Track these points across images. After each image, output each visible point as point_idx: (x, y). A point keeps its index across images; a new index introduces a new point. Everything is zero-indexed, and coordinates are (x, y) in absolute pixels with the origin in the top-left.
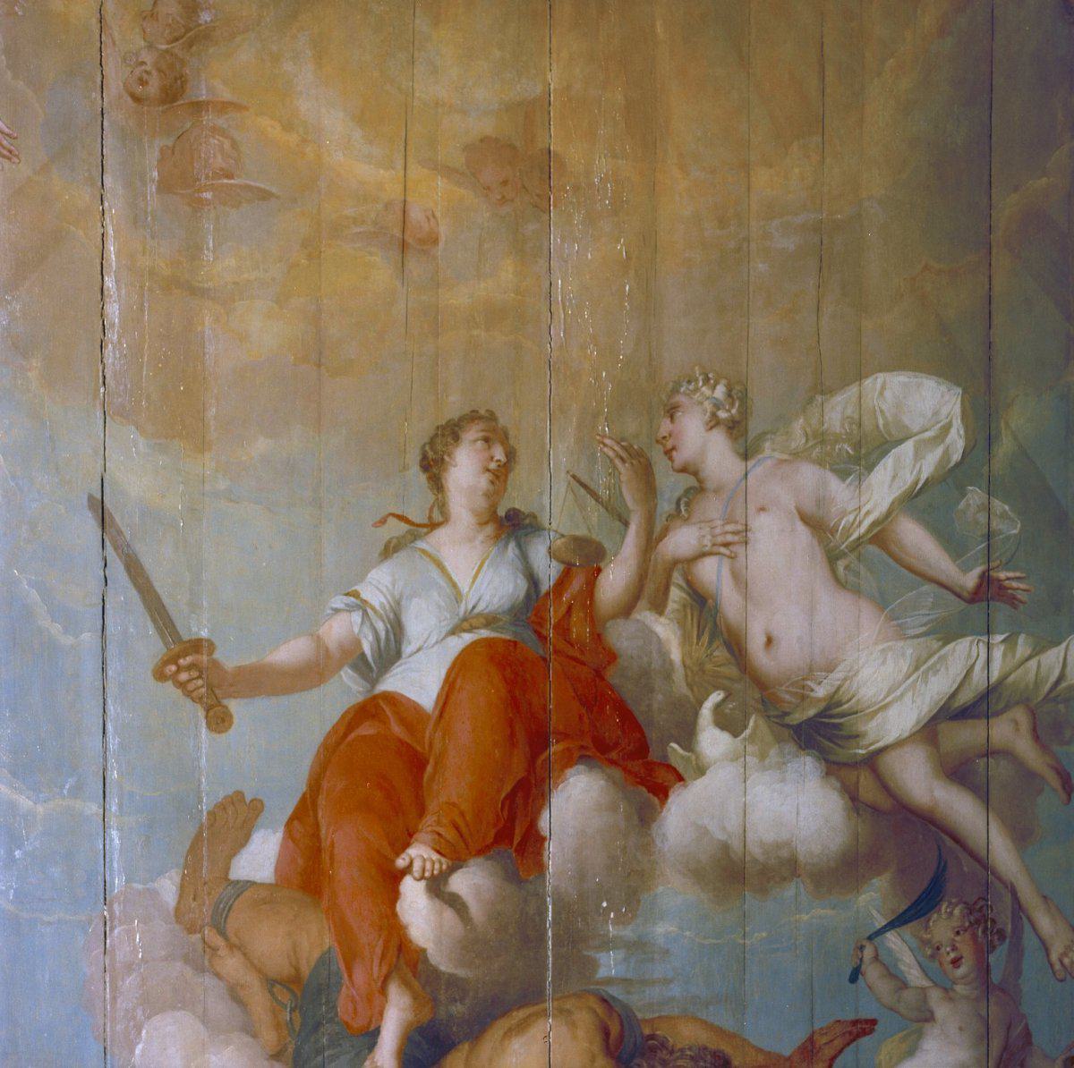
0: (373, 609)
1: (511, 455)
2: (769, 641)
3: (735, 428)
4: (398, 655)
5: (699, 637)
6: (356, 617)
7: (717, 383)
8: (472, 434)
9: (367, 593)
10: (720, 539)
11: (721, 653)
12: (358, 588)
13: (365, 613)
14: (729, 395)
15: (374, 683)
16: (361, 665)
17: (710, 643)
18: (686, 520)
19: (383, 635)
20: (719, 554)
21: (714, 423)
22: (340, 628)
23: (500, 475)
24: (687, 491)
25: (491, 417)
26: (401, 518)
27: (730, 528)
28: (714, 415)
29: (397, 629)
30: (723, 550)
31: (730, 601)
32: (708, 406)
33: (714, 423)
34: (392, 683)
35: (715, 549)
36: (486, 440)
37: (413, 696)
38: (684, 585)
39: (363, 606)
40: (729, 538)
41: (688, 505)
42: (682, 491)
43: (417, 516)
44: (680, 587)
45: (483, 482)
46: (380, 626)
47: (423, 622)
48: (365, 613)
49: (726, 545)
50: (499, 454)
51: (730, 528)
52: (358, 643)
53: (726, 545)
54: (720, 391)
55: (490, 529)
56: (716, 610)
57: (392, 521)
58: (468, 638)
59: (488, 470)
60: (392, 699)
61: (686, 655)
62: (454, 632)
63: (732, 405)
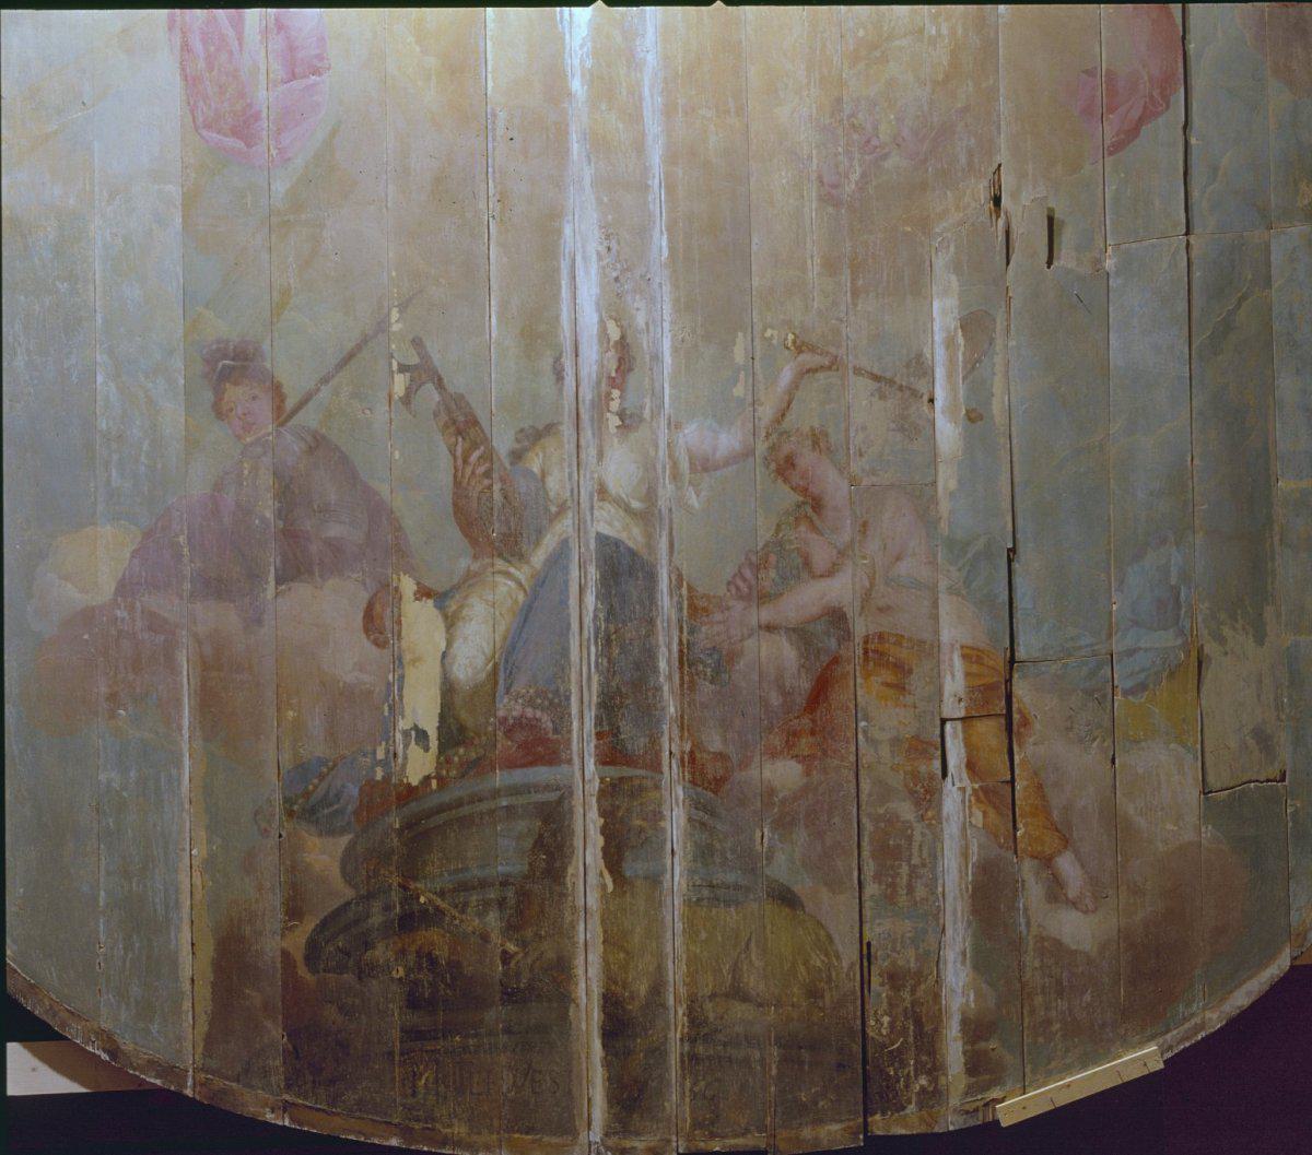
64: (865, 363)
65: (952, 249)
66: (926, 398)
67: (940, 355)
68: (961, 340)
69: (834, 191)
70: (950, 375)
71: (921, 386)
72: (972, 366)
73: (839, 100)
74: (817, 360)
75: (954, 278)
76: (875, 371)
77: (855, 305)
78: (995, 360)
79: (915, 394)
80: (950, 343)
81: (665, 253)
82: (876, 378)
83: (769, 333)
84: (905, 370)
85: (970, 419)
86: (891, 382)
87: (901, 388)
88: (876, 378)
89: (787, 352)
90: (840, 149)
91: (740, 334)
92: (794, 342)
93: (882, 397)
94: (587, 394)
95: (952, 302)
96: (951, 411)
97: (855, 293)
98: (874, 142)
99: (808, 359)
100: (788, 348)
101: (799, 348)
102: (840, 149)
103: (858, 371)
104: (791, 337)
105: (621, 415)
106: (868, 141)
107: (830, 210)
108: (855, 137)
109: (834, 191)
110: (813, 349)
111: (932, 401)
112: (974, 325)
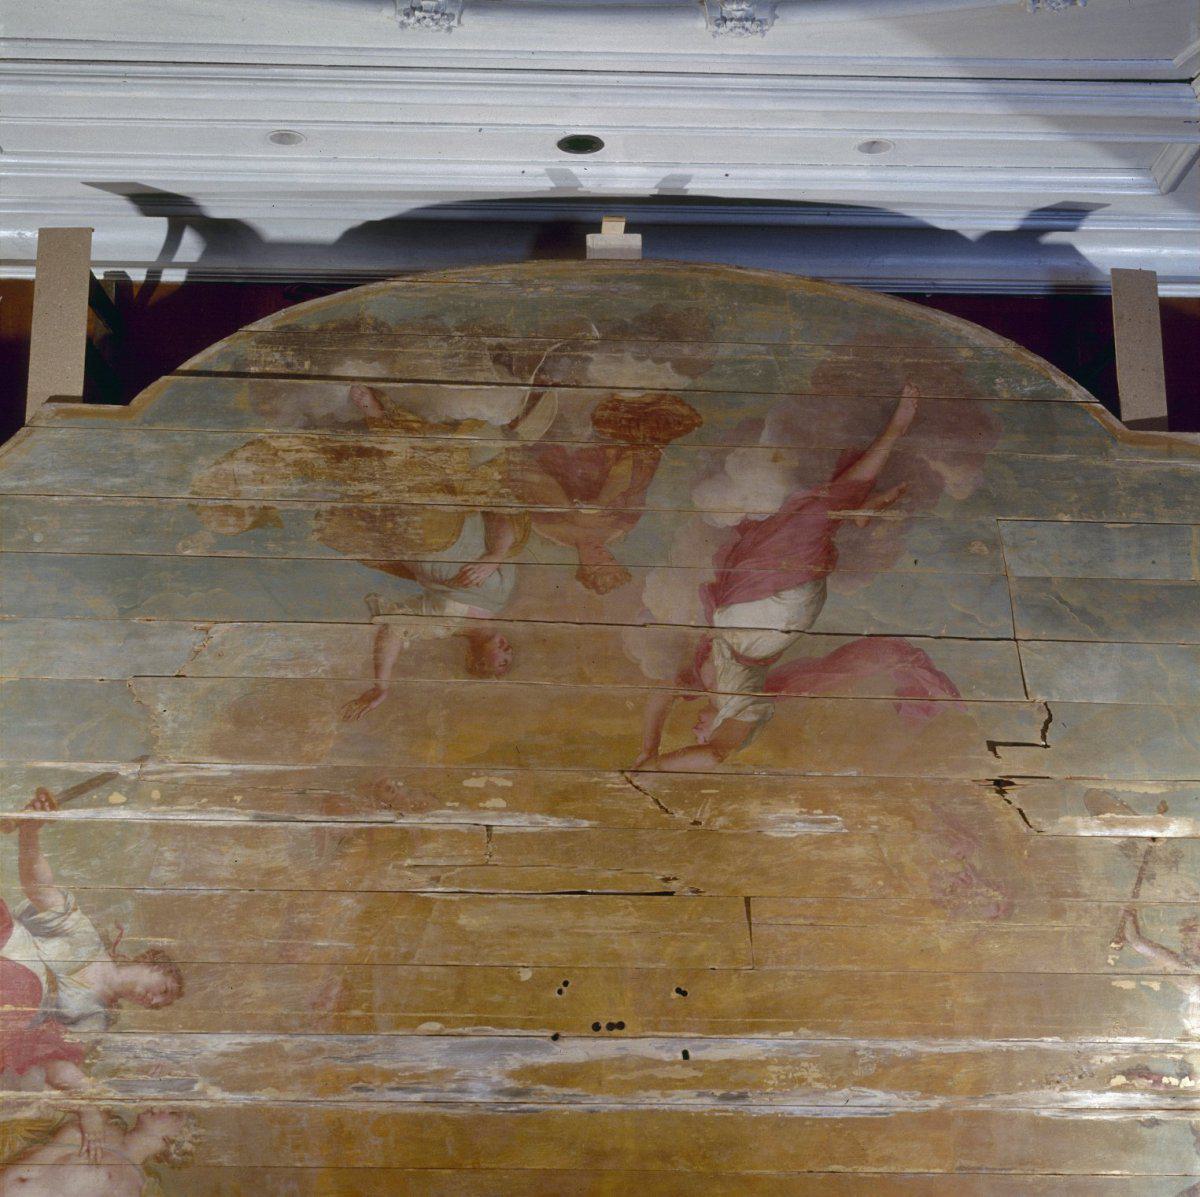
0: (65, 920)
1: (157, 1007)
2: (23, 1180)
3: (163, 1157)
4: (35, 935)
5: (29, 1131)
6: (61, 909)
7: (194, 1144)
8: (171, 983)
9: (75, 916)
10: (92, 1146)
11: (19, 1145)
12: (79, 911)
13: (63, 914)
14: (185, 1153)
15: (20, 919)
16: (31, 911)
17: (25, 1138)
18: (106, 1123)
19: (49, 925)
20: (83, 1145)
21: (168, 1141)
22: (56, 899)
23: (143, 1000)
24: (125, 1124)
25: (180, 994)
26: (121, 935)
27: (99, 1153)
28: (173, 1142)
29: (53, 934)
30: (85, 1148)
31: (52, 1153)
32: (178, 1139)
33: (168, 1141)
34: (18, 931)
35: (86, 1143)
36: (165, 992)
37: (11, 942)
38: (65, 1121)
39: (66, 913)
40: (92, 1153)
41: (116, 1124)
42: (125, 1120)
43: (120, 949)
44: (64, 1118)
45: (139, 989)
46: (55, 923)
47: (53, 949)
48: (63, 914)
49: (88, 1151)
50: (156, 1000)
51: (99, 1153)
52: (44, 909)
53: (88, 1151)
54: (188, 1146)
55: (110, 993)
56: (45, 1144)
57: (117, 933)
58: (43, 979)
59: (147, 992)
61: (18, 1121)
62: (49, 971)
63: (178, 1155)
64: (1129, 889)
65: (1040, 820)
66: (1151, 844)
67: (1119, 832)
68: (1108, 815)
69: (1002, 908)
70: (1135, 825)
71: (1142, 847)
72: (1126, 808)
73: (933, 902)
74: (1129, 925)
75: (1063, 819)
76: (1134, 881)
77: (1085, 896)
78: (1120, 790)
79: (1149, 852)
80: (1110, 824)
81: (1056, 1039)
82: (1139, 881)
83: (1111, 962)
84: (1132, 859)
85: (1165, 811)
86: (1142, 869)
87: (1146, 863)
88: (1139, 881)
89: (1125, 948)
90: (970, 903)
91: (1114, 983)
92: (1117, 943)
93: (1153, 876)
94: (1167, 1102)
95: (1079, 821)
96: (1161, 825)
97: (1077, 895)
98: (962, 876)
99: (1129, 932)
100: (1121, 948)
101: (1120, 938)
102: (970, 903)
103: (1135, 895)
104: (1113, 945)
105: (1181, 1076)
106: (962, 880)
107: (1016, 911)
108: (959, 890)
109: (1002, 908)
110: (1122, 928)
111: (1154, 839)
112: (1096, 805)
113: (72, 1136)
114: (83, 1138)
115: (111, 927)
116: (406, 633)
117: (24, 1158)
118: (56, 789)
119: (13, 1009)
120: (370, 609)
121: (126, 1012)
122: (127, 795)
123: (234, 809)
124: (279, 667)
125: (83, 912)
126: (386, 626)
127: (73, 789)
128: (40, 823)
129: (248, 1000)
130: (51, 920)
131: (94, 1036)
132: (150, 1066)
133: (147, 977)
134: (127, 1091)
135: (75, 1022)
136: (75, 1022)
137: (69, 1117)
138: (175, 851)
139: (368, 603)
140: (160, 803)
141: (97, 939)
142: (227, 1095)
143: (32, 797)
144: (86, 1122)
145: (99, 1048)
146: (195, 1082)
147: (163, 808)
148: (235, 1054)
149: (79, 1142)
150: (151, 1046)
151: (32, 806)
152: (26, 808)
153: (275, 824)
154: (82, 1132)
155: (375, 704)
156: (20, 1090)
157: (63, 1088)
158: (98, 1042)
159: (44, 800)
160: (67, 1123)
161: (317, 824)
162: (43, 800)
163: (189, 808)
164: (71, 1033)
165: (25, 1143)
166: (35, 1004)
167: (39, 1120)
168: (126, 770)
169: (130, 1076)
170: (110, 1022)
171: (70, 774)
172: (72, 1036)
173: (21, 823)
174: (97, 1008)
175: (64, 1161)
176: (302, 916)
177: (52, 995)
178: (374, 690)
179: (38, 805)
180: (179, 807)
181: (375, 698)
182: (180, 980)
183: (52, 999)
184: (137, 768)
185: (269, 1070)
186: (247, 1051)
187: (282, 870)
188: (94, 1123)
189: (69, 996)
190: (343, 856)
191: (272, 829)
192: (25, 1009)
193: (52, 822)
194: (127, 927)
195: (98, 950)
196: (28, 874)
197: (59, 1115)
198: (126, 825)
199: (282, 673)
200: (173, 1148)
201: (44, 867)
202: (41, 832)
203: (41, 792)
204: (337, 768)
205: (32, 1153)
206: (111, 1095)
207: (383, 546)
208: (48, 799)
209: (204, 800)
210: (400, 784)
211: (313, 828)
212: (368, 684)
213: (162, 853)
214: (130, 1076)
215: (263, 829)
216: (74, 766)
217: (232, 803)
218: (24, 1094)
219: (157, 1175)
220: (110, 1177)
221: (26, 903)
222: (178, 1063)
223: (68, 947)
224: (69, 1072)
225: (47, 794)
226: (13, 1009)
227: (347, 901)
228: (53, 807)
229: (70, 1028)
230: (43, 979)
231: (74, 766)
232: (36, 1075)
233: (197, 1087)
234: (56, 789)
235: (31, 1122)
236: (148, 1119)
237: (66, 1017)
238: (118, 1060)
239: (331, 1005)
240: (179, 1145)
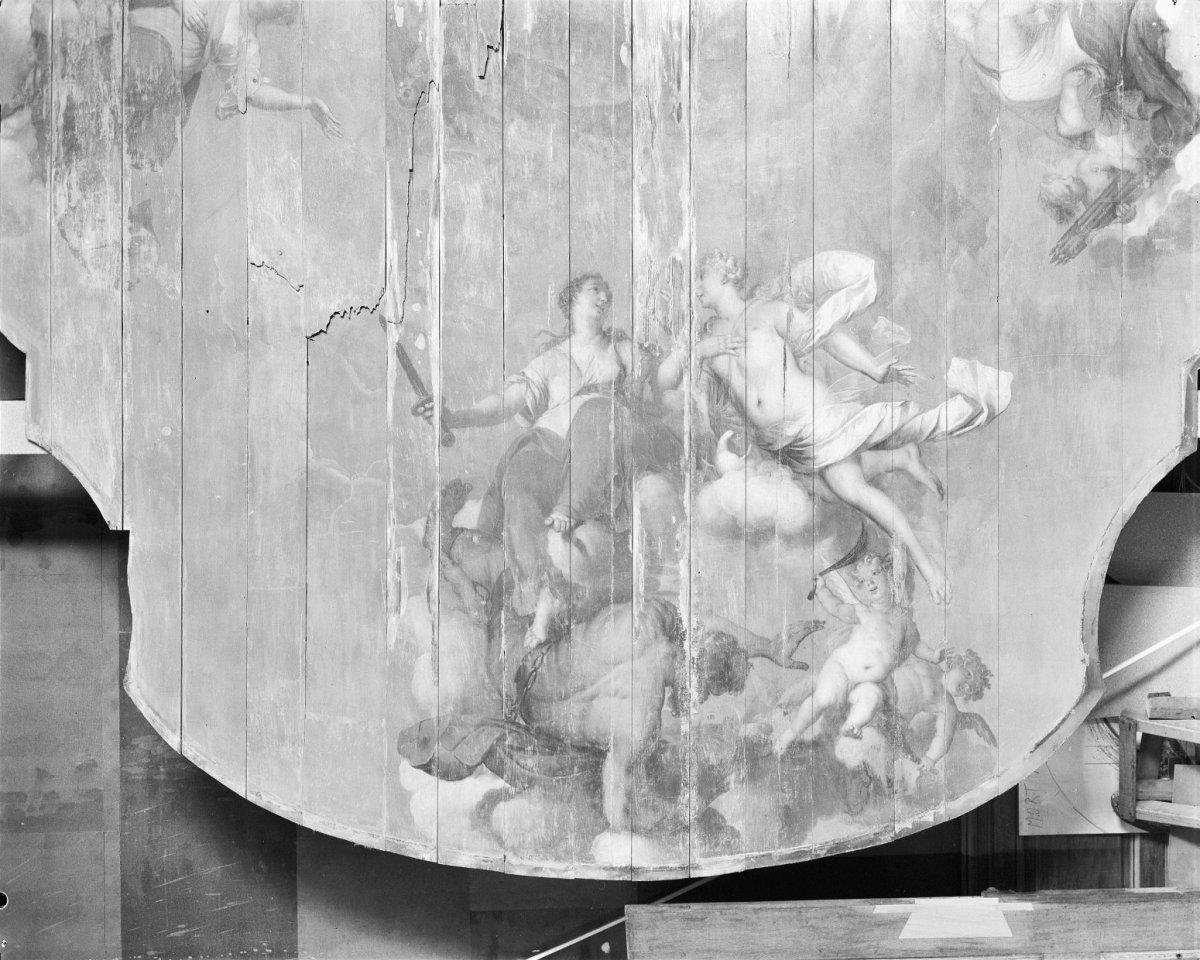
1: (609, 297)
3: (739, 284)
6: (523, 386)
9: (529, 373)
10: (730, 346)
11: (730, 409)
12: (525, 371)
13: (528, 384)
16: (526, 413)
19: (538, 396)
22: (514, 392)
30: (732, 351)
31: (737, 382)
34: (543, 422)
39: (527, 382)
40: (736, 345)
47: (559, 391)
49: (734, 349)
53: (734, 349)
54: (730, 263)
55: (598, 337)
60: (539, 430)
61: (710, 410)
113: (722, 364)
114: (724, 353)
115: (539, 341)
116: (255, 81)
117: (741, 404)
118: (413, 397)
119: (612, 422)
120: (231, 115)
121: (616, 322)
122: (416, 334)
123: (429, 236)
124: (291, 200)
125: (526, 366)
126: (248, 100)
127: (412, 382)
128: (445, 412)
129: (602, 217)
130: (534, 394)
131: (636, 350)
132: (662, 300)
133: (585, 305)
134: (683, 319)
135: (623, 368)
136: (623, 368)
137: (705, 368)
138: (468, 288)
139: (225, 118)
140: (424, 302)
141: (550, 352)
142: (686, 231)
143: (421, 419)
144: (710, 352)
145: (646, 345)
146: (674, 259)
147: (429, 300)
148: (650, 226)
149: (726, 357)
150: (644, 300)
151: (429, 419)
152: (431, 423)
153: (442, 197)
154: (719, 355)
155: (326, 109)
156: (683, 412)
157: (681, 374)
158: (641, 346)
159: (422, 408)
160: (710, 368)
161: (441, 159)
162: (423, 408)
163: (428, 276)
164: (633, 370)
165: (729, 403)
166: (609, 403)
167: (709, 393)
168: (394, 335)
169: (670, 317)
170: (622, 337)
171: (399, 386)
172: (636, 370)
173: (445, 427)
174: (611, 348)
175: (744, 371)
176: (526, 171)
177: (600, 389)
178: (312, 110)
179: (428, 413)
180: (428, 286)
181: (320, 110)
182: (586, 277)
183: (603, 389)
184: (391, 327)
185: (663, 195)
186: (647, 215)
187: (484, 187)
188: (710, 345)
189: (600, 374)
190: (470, 134)
191: (446, 201)
192: (613, 412)
193: (444, 400)
194: (538, 327)
195: (559, 351)
196: (492, 418)
197: (705, 376)
198: (445, 334)
199: (297, 196)
200: (731, 276)
201: (486, 404)
202: (453, 409)
203: (415, 412)
204: (388, 142)
205: (736, 397)
206: (687, 332)
207: (167, 104)
208: (423, 404)
209: (421, 263)
210: (402, 84)
211: (445, 163)
212: (307, 116)
213: (471, 299)
214: (670, 317)
215: (446, 208)
216: (391, 383)
217: (423, 238)
218: (686, 408)
219: (754, 288)
220: (755, 329)
221: (518, 418)
222: (658, 275)
223: (557, 378)
224: (667, 370)
225: (418, 406)
226: (612, 422)
227: (511, 130)
228: (430, 400)
229: (629, 371)
230: (586, 397)
231: (391, 383)
232: (670, 397)
233: (679, 258)
234: (413, 397)
235: (710, 399)
236: (706, 300)
237: (620, 375)
238: (656, 329)
239: (606, 143)
240: (728, 271)
